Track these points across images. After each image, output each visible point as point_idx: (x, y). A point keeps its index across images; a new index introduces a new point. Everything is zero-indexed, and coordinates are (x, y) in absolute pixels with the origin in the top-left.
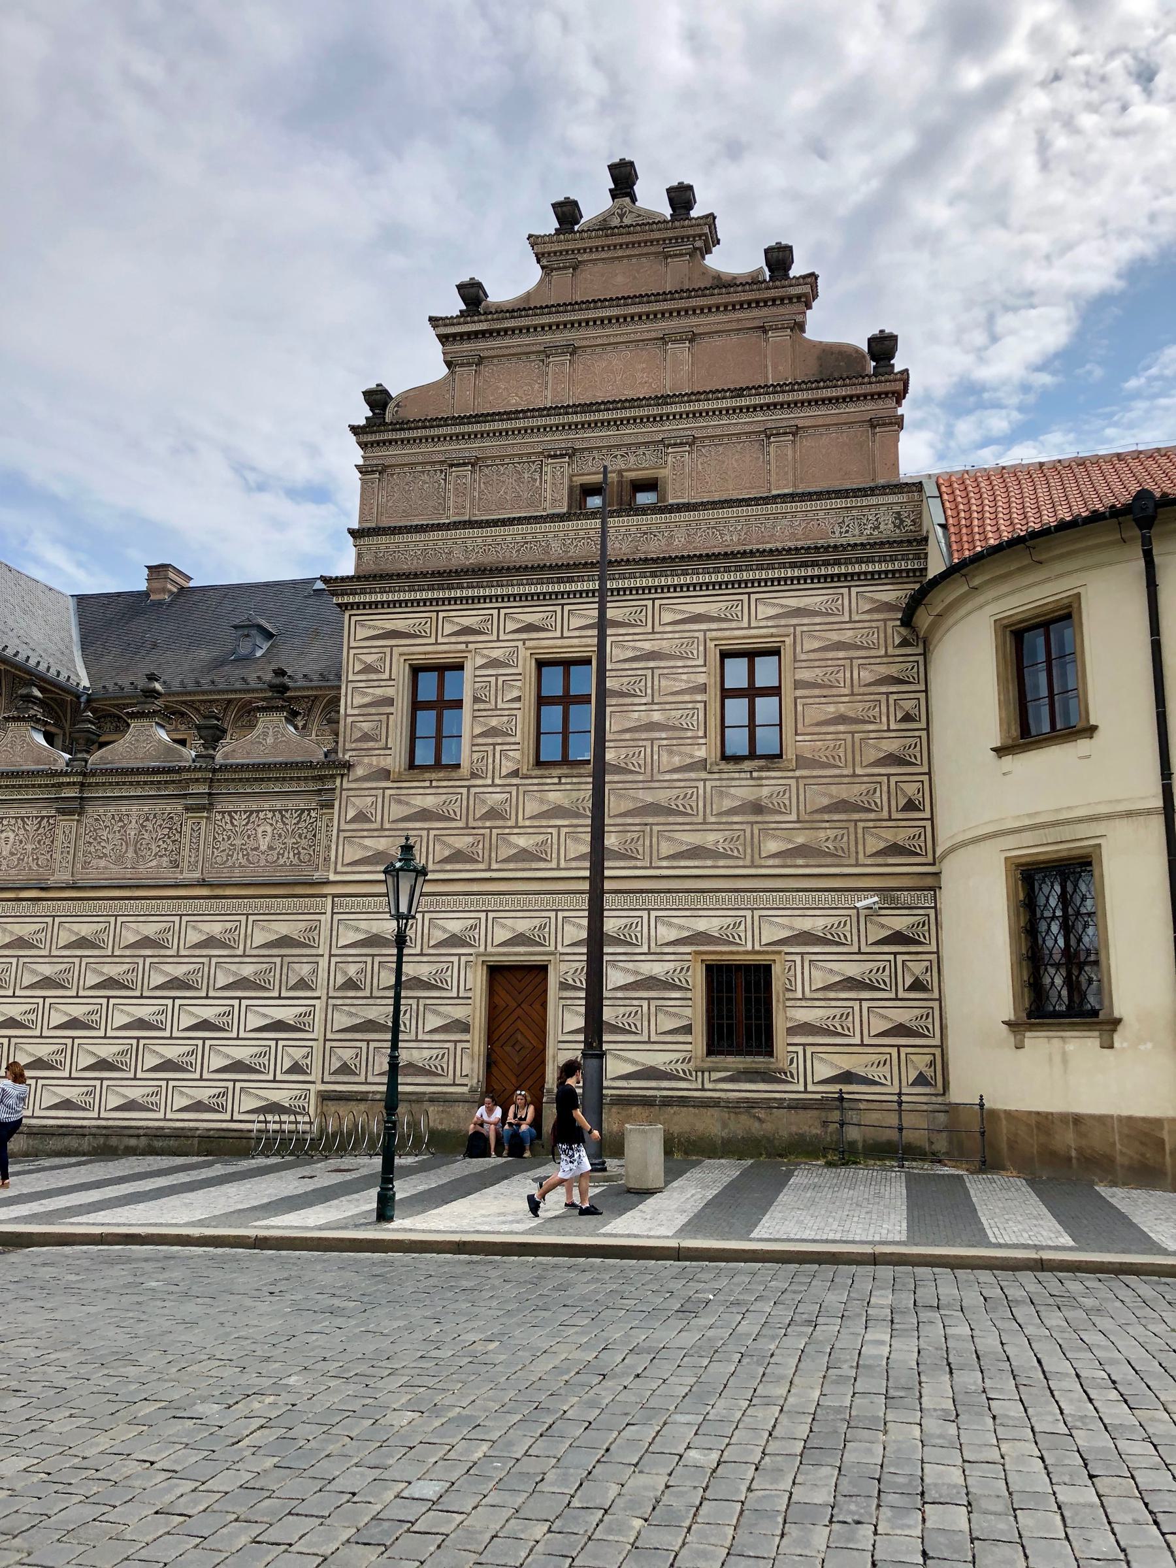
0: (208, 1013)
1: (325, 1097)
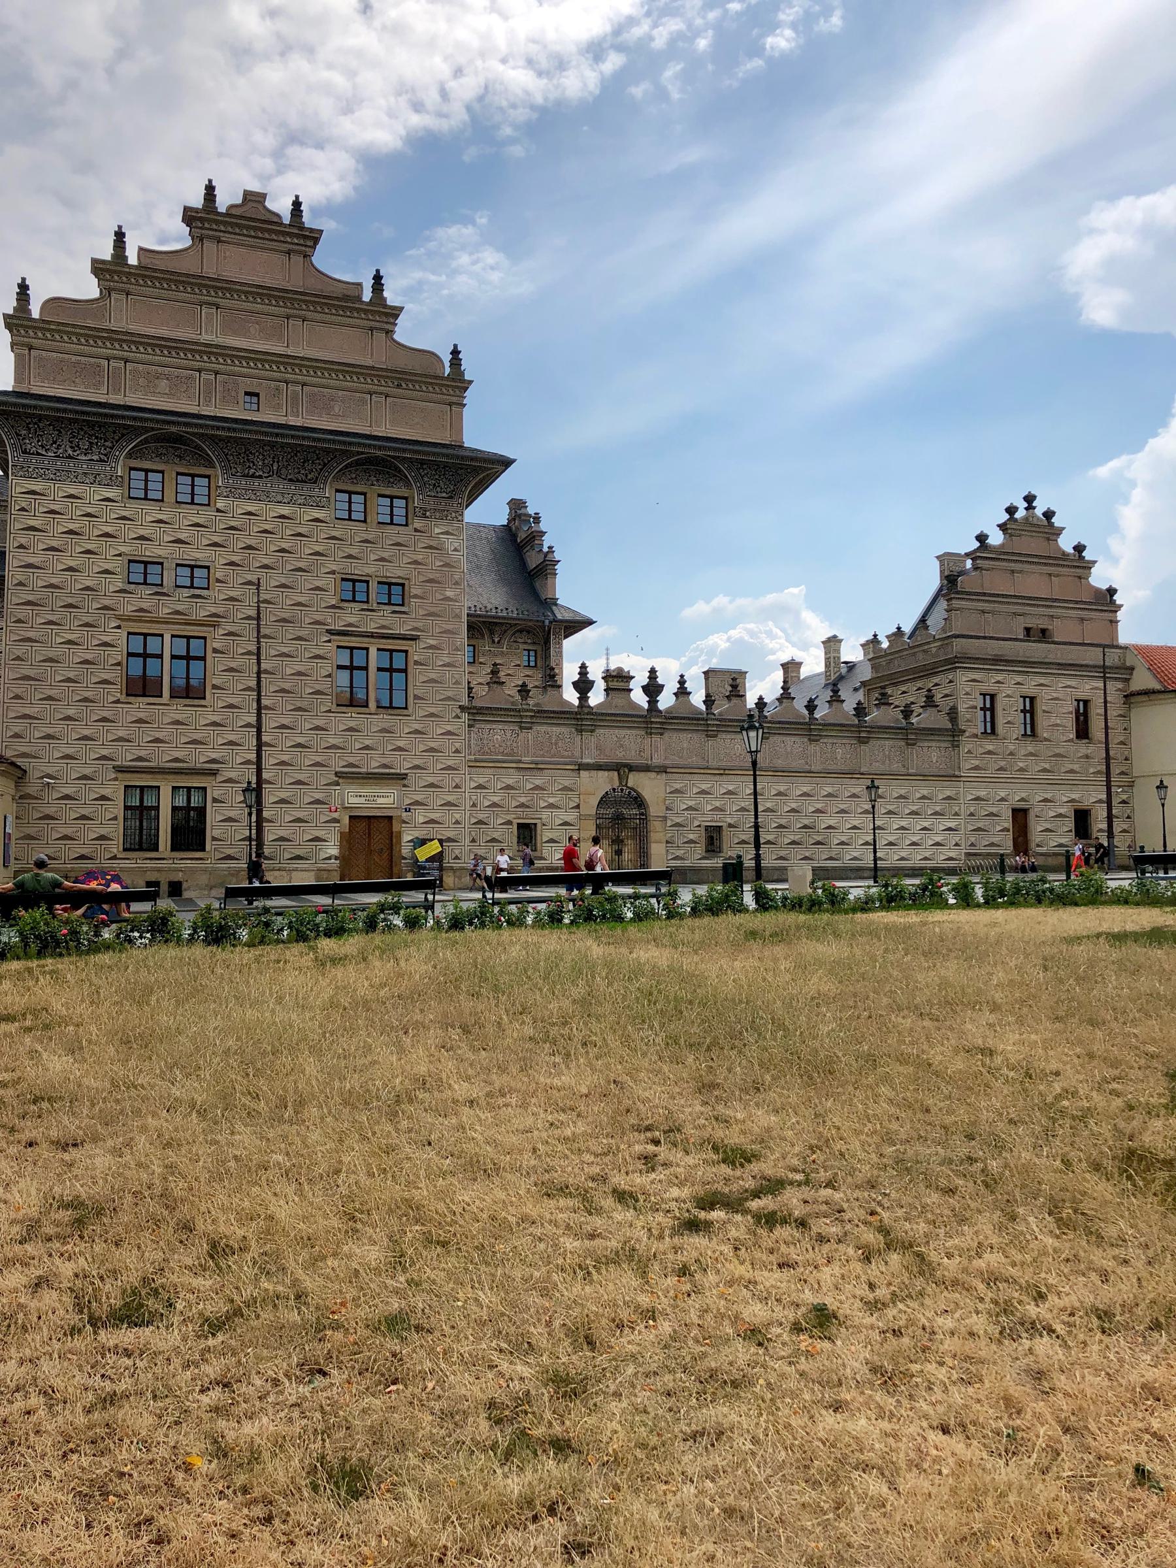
0: (926, 824)
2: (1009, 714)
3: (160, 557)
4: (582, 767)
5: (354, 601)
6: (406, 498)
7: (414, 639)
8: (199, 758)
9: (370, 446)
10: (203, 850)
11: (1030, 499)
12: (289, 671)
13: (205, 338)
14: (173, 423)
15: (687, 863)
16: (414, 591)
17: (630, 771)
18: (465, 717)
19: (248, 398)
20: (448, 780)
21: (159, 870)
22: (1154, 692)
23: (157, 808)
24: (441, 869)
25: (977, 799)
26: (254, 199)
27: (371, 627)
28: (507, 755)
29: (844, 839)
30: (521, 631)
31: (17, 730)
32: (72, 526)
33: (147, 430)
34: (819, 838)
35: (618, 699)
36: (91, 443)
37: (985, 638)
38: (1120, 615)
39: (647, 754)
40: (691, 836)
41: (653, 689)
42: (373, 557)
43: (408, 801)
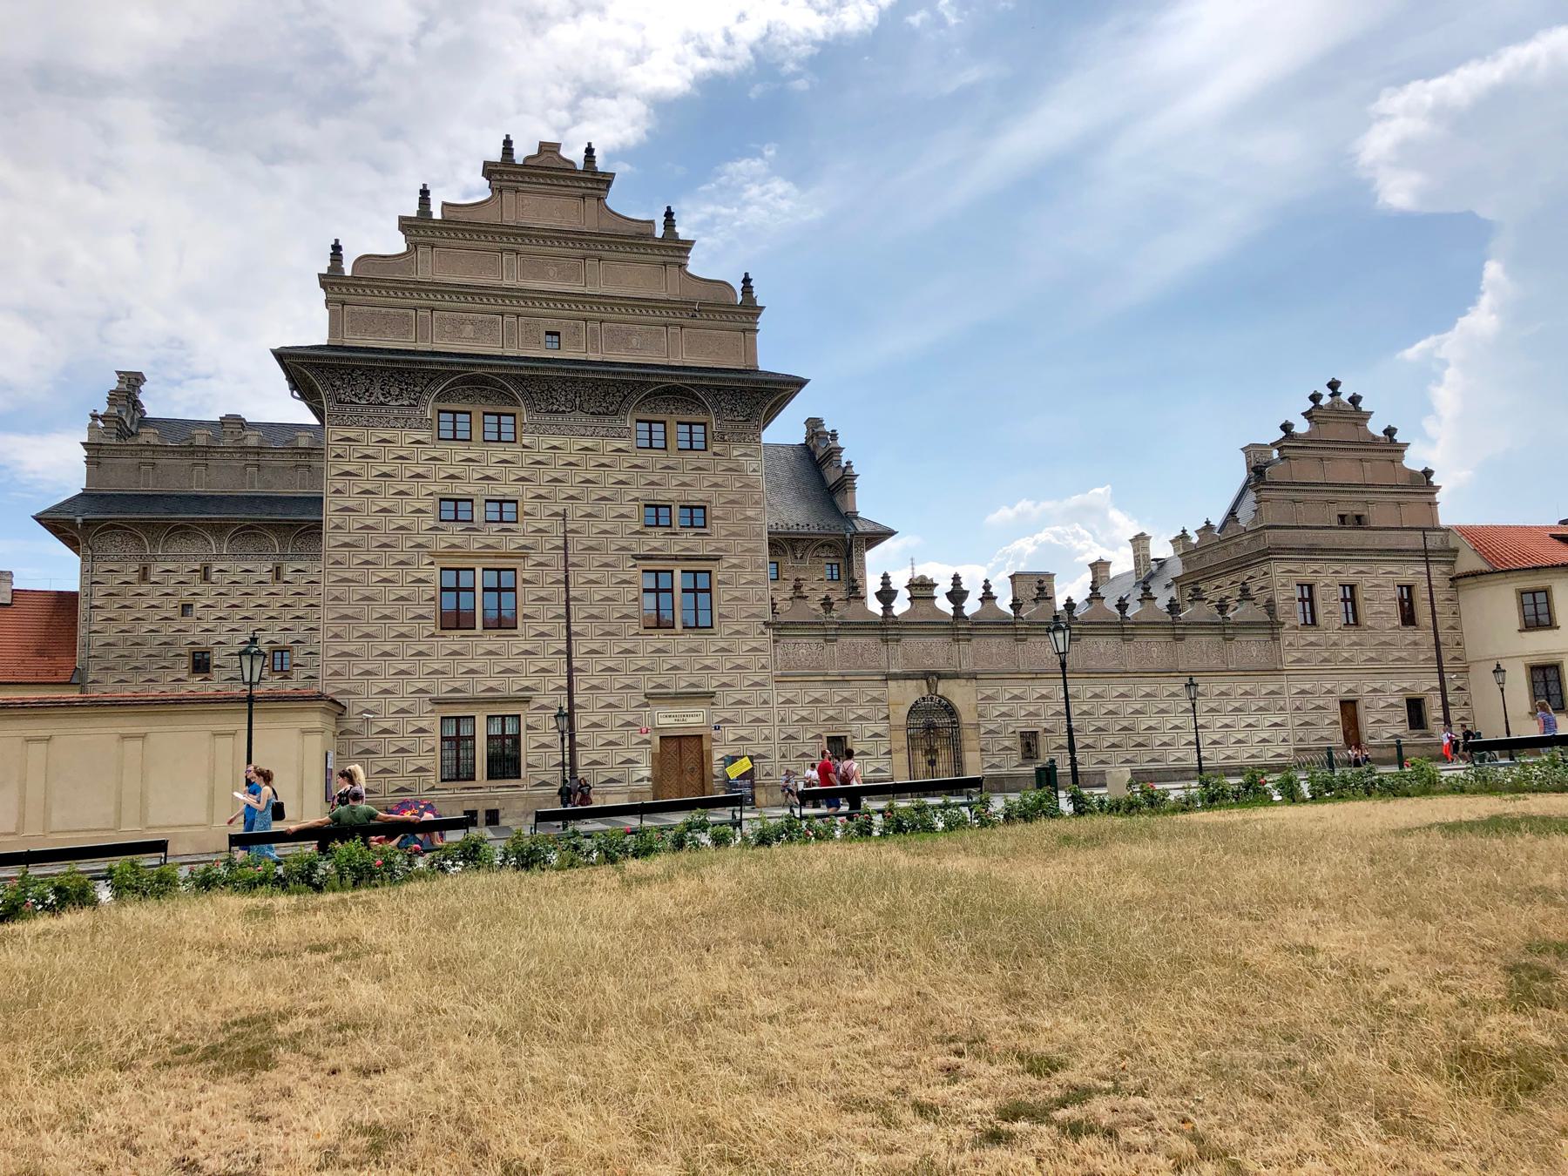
0: (1250, 721)
1: (1297, 750)
2: (1329, 605)
3: (469, 494)
4: (889, 677)
5: (657, 525)
6: (704, 424)
7: (717, 559)
8: (513, 686)
9: (667, 376)
10: (519, 777)
11: (1334, 385)
12: (597, 597)
13: (506, 283)
14: (480, 365)
15: (1004, 771)
16: (716, 513)
17: (938, 679)
18: (770, 632)
19: (549, 338)
20: (756, 695)
21: (476, 799)
22: (1482, 573)
23: (473, 738)
24: (752, 786)
25: (1303, 692)
26: (549, 149)
27: (676, 550)
28: (813, 668)
29: (1166, 739)
30: (823, 546)
31: (336, 667)
32: (385, 469)
33: (454, 373)
34: (1140, 740)
35: (923, 607)
36: (401, 389)
37: (1298, 527)
38: (1438, 497)
39: (955, 661)
40: (1007, 743)
41: (957, 595)
42: (675, 482)
43: (717, 719)
